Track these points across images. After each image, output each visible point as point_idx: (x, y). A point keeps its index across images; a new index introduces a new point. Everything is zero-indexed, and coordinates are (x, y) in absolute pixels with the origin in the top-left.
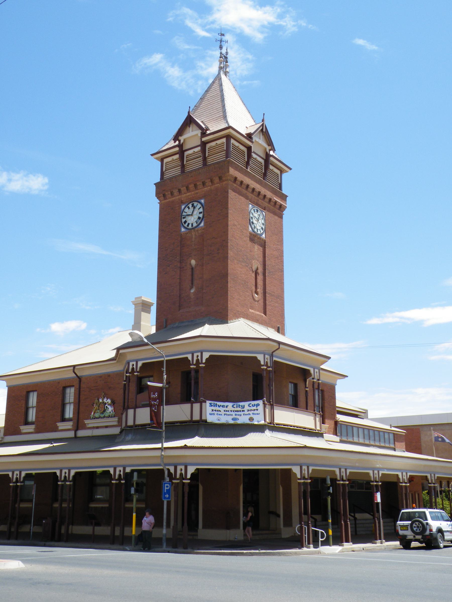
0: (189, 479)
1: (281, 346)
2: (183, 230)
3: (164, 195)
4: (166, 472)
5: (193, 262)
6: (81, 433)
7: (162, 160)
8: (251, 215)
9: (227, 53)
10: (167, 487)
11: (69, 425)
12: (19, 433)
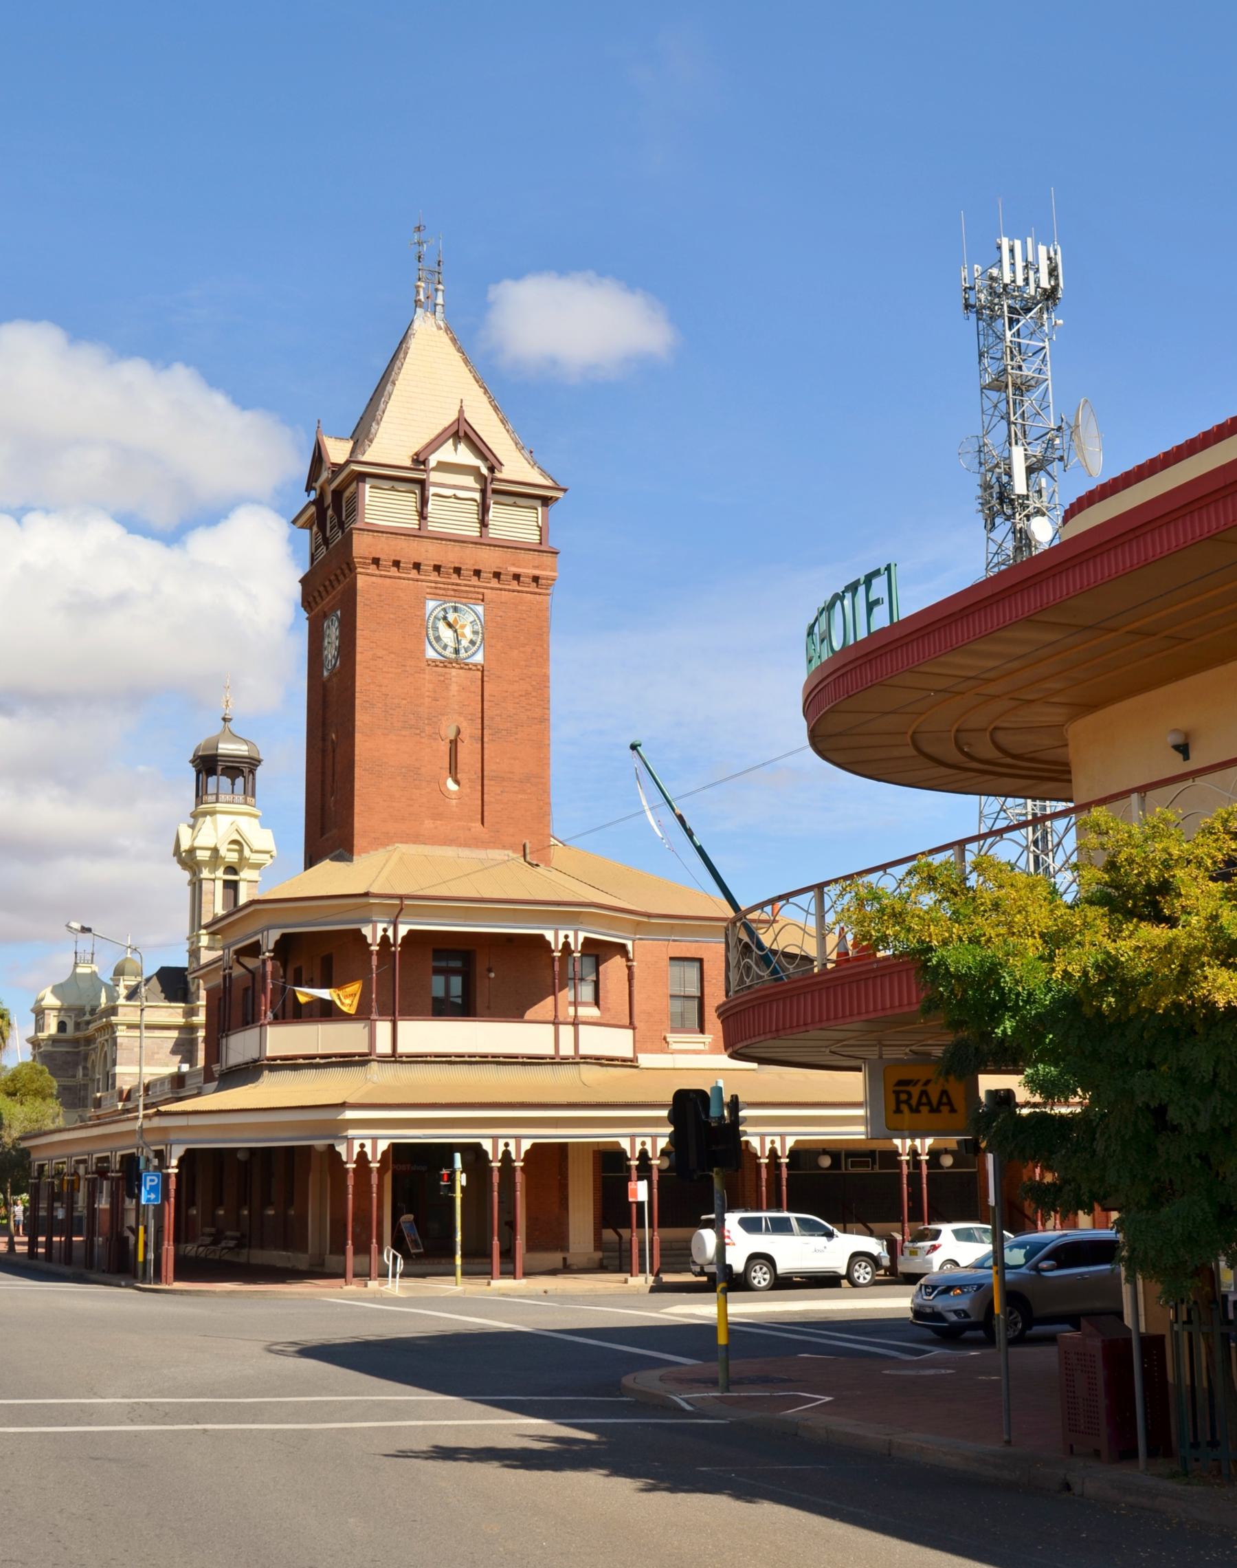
0: (177, 1167)
1: (407, 902)
2: (326, 674)
7: (311, 529)
10: (152, 1181)
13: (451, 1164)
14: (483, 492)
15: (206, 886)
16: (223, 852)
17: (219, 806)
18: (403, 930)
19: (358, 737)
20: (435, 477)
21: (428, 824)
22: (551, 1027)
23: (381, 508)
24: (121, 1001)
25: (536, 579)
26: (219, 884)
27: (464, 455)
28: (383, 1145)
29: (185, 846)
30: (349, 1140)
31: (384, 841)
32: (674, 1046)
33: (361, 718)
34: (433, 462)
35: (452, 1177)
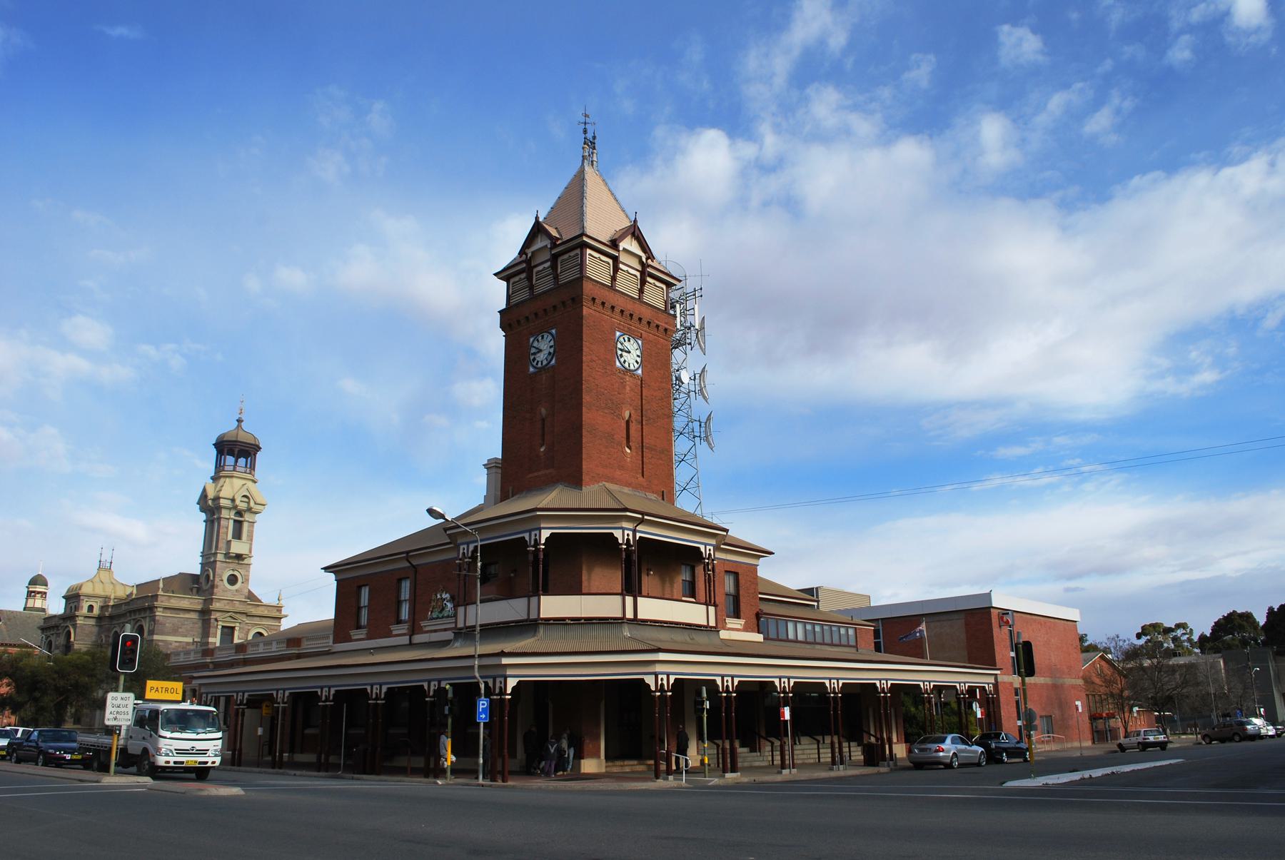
2: (532, 369)
3: (510, 325)
4: (482, 686)
5: (543, 411)
6: (418, 638)
8: (619, 346)
9: (594, 138)
11: (403, 629)
12: (349, 639)
13: (700, 694)
14: (643, 273)
15: (223, 522)
16: (238, 502)
17: (235, 474)
18: (638, 535)
19: (584, 409)
20: (623, 258)
21: (618, 473)
22: (704, 607)
23: (596, 267)
24: (160, 592)
25: (666, 330)
26: (231, 522)
27: (634, 247)
28: (672, 679)
29: (211, 494)
30: (656, 675)
31: (597, 479)
32: (729, 626)
33: (586, 398)
34: (622, 245)
35: (703, 703)
